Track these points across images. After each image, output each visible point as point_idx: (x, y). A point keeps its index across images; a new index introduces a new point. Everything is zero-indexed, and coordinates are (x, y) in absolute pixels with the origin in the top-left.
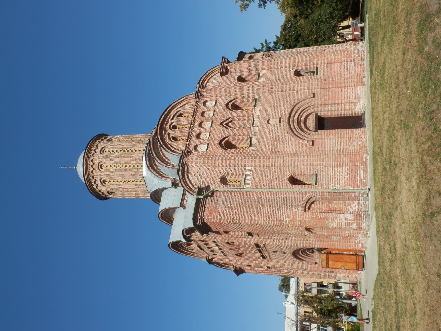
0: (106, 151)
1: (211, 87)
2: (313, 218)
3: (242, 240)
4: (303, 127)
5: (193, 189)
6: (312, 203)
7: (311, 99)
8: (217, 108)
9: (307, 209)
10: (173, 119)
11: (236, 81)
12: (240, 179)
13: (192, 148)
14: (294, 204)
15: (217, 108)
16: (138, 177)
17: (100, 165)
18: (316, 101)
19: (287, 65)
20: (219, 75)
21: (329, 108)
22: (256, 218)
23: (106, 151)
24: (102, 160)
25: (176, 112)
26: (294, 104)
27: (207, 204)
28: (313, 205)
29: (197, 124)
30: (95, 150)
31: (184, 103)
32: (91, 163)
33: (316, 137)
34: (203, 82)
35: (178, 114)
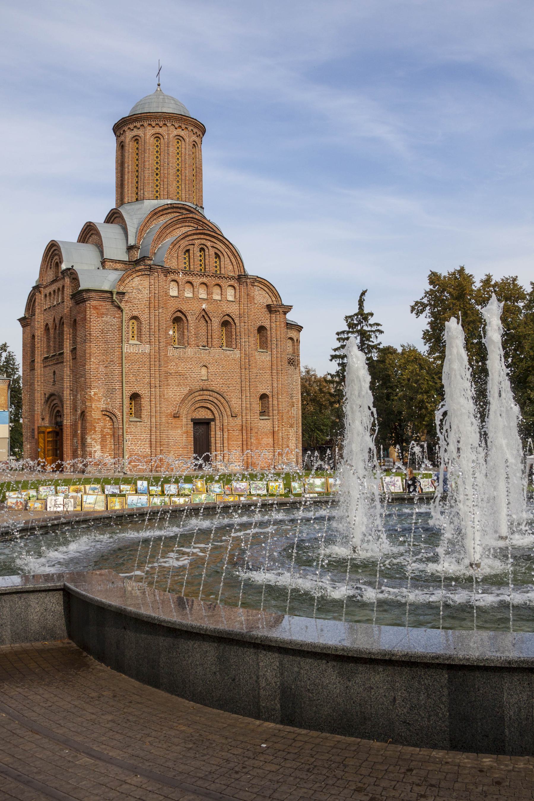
0: (178, 142)
1: (252, 294)
3: (67, 339)
4: (197, 405)
6: (111, 418)
7: (229, 413)
8: (224, 303)
9: (104, 413)
10: (212, 247)
11: (259, 324)
12: (136, 339)
13: (172, 276)
14: (109, 400)
15: (224, 303)
16: (142, 191)
17: (159, 136)
19: (275, 385)
21: (219, 433)
22: (92, 360)
23: (178, 142)
24: (166, 140)
25: (222, 251)
26: (225, 395)
27: (107, 303)
28: (108, 419)
29: (205, 280)
30: (180, 127)
31: (233, 260)
32: (161, 124)
33: (184, 420)
34: (260, 282)
35: (219, 253)
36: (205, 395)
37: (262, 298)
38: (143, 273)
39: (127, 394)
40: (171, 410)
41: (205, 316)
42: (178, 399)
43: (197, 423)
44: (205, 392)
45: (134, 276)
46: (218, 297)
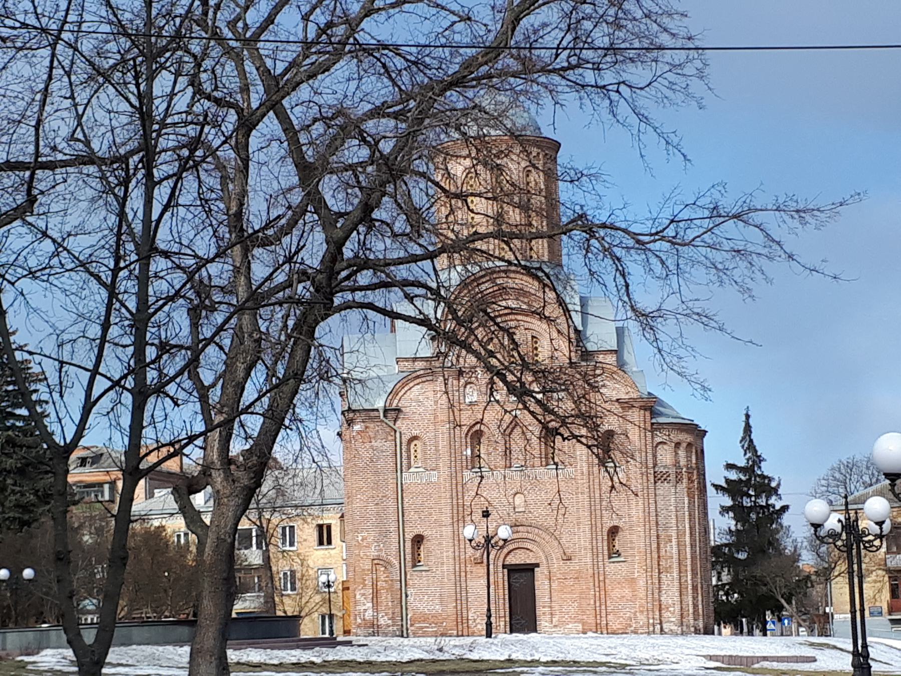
2: (364, 570)
5: (398, 398)
9: (376, 562)
18: (557, 565)
21: (547, 582)
38: (424, 379)
39: (409, 536)
44: (520, 528)
45: (411, 385)
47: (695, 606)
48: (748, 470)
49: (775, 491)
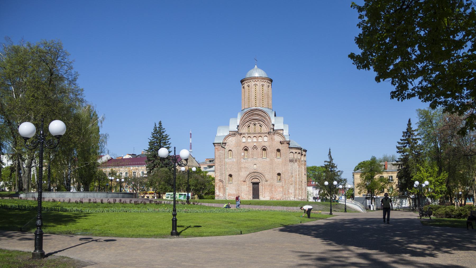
13: (243, 135)
20: (282, 140)
29: (255, 135)
36: (255, 174)
37: (278, 138)
40: (242, 179)
41: (255, 147)
42: (245, 176)
43: (254, 184)
46: (261, 141)
47: (299, 193)
48: (330, 162)
49: (336, 167)
